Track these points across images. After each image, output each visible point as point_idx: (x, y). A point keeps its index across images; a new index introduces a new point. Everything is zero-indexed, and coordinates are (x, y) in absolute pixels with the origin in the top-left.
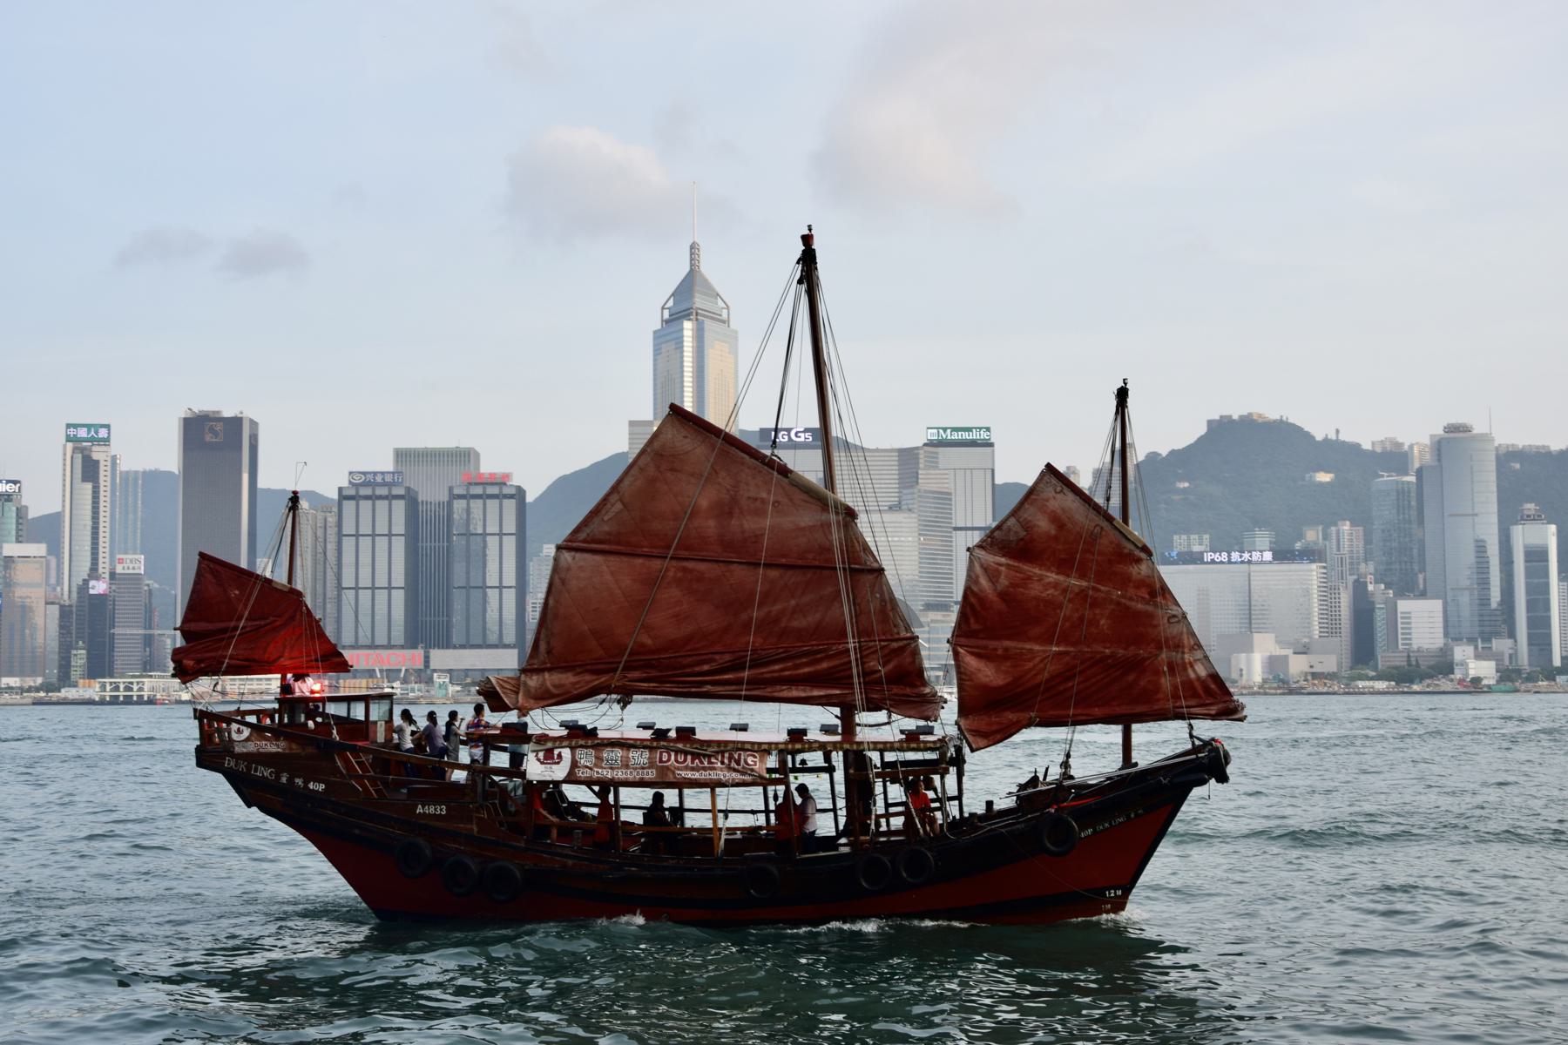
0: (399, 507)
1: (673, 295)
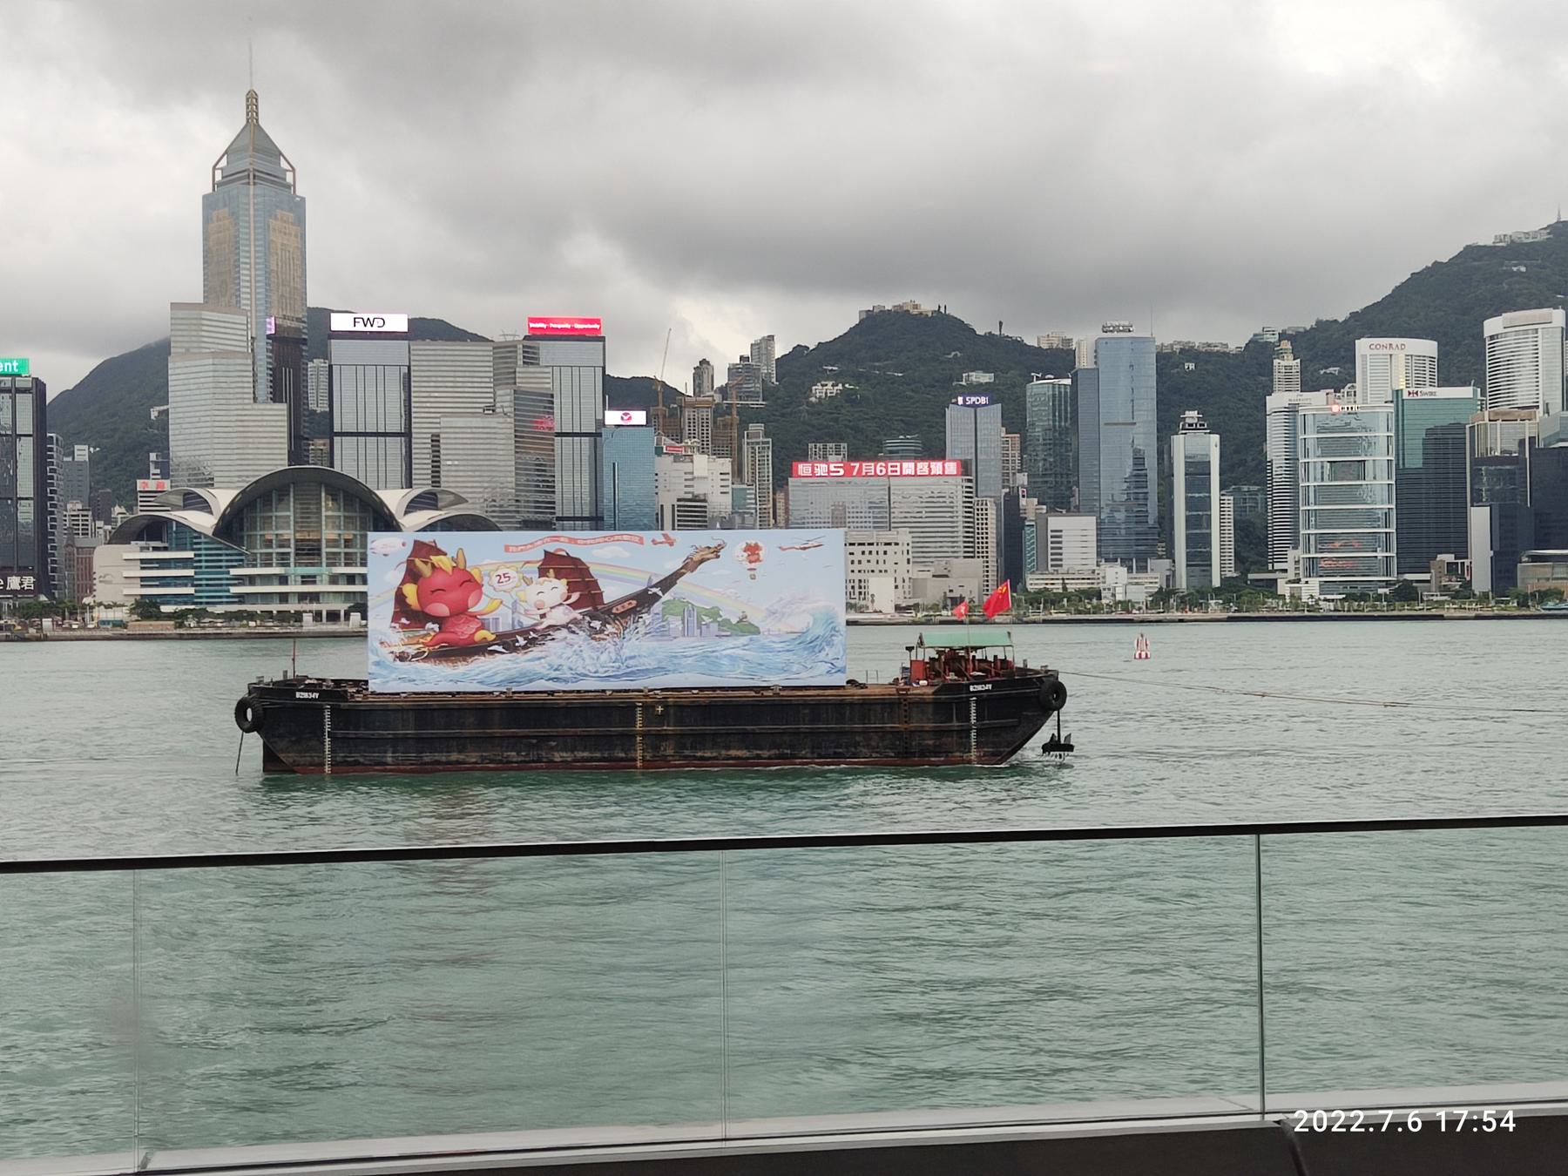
1: (226, 152)
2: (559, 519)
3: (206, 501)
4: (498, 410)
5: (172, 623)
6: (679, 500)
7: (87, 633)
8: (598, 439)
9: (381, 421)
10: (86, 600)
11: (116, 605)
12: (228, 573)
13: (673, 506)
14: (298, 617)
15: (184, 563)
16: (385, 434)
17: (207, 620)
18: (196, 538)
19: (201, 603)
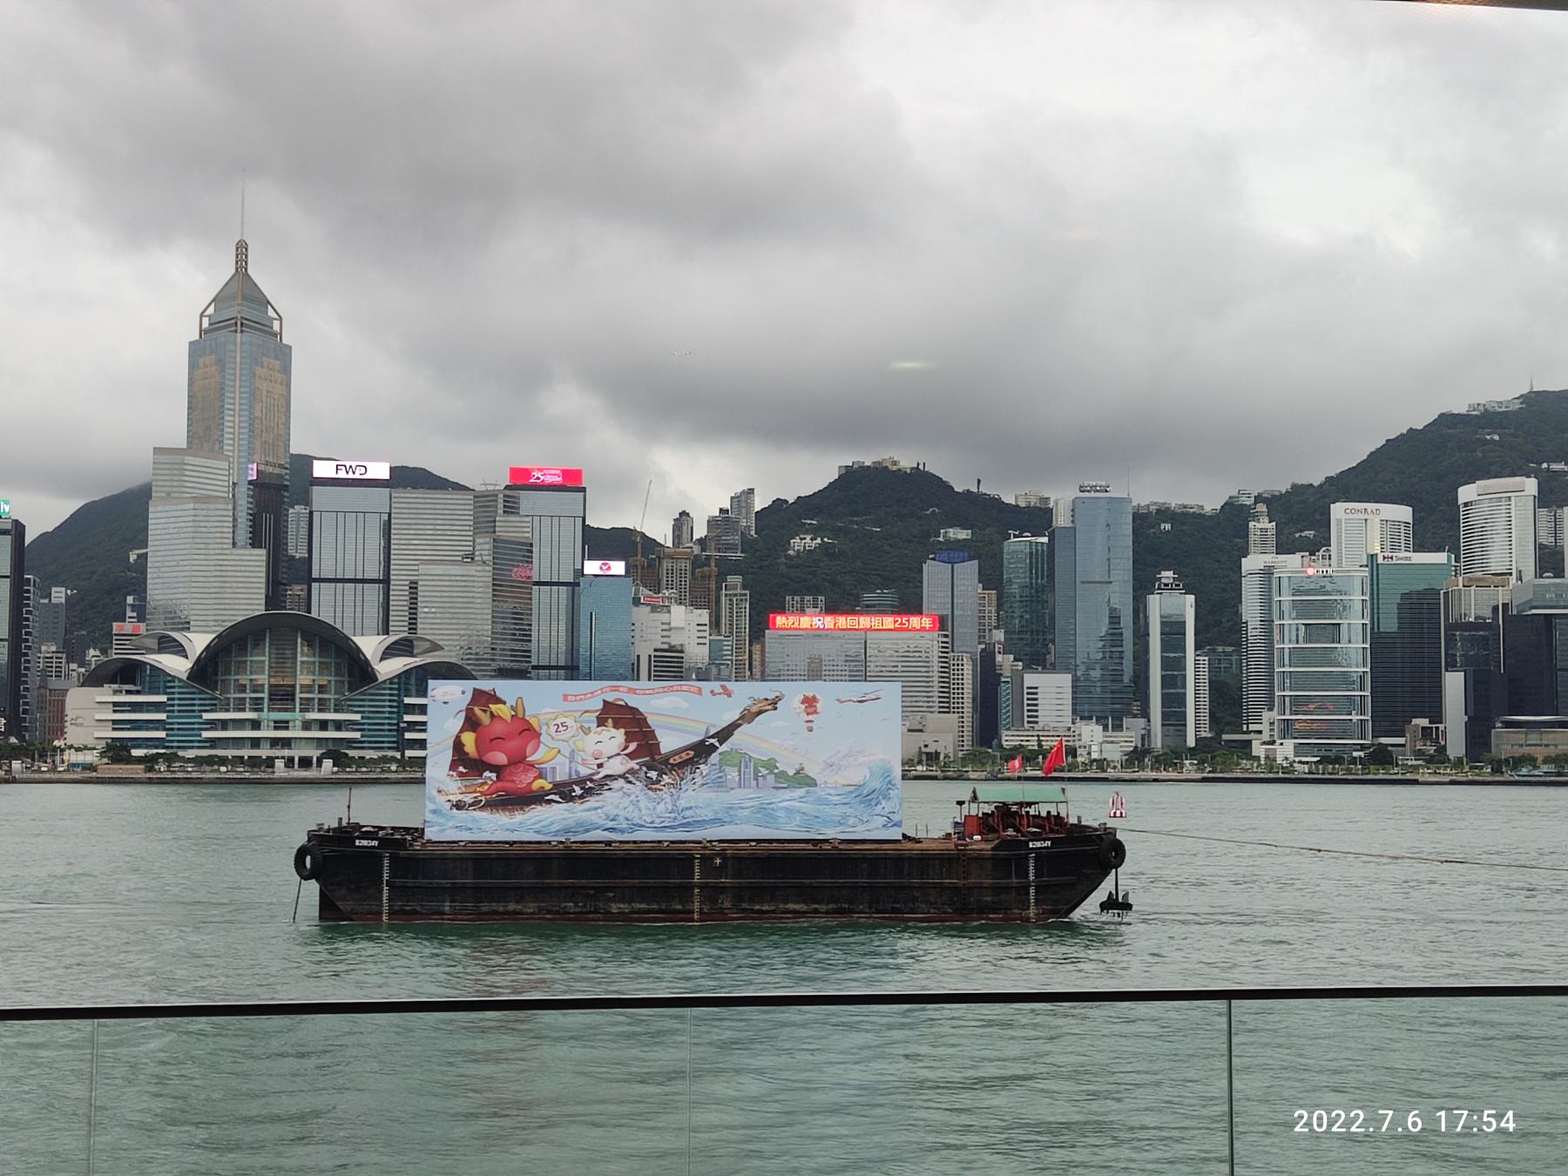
1: (214, 300)
2: (534, 667)
3: (181, 645)
4: (476, 558)
5: (142, 767)
6: (655, 650)
7: (56, 776)
8: (576, 588)
9: (360, 568)
10: (56, 743)
11: (86, 748)
12: (201, 717)
13: (650, 656)
14: (270, 762)
15: (157, 707)
16: (363, 581)
18: (169, 681)
19: (172, 747)
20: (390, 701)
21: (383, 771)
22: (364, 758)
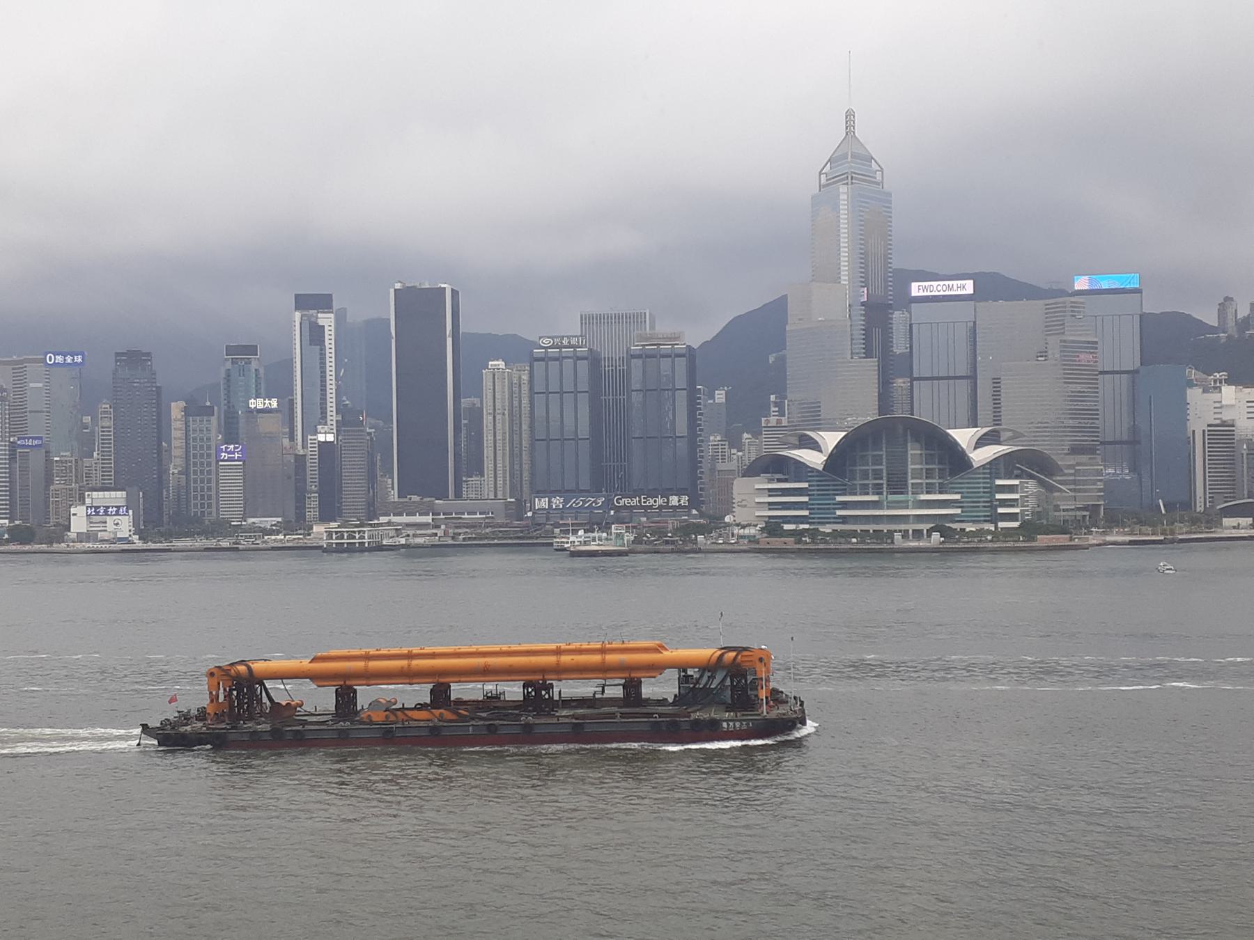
0: (583, 367)
3: (817, 442)
5: (793, 539)
10: (727, 519)
11: (749, 525)
17: (820, 537)
18: (810, 472)
19: (814, 523)
20: (984, 483)
21: (980, 541)
22: (964, 529)
